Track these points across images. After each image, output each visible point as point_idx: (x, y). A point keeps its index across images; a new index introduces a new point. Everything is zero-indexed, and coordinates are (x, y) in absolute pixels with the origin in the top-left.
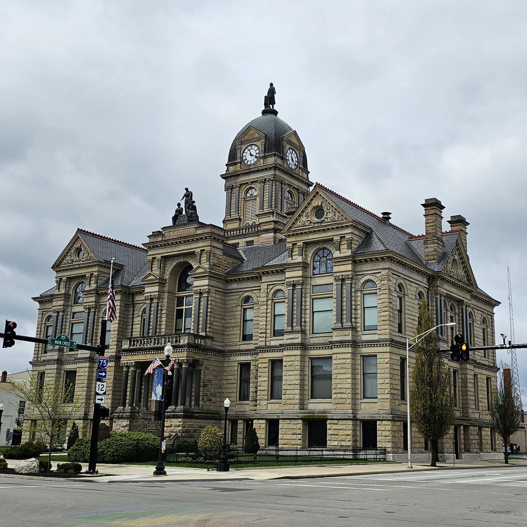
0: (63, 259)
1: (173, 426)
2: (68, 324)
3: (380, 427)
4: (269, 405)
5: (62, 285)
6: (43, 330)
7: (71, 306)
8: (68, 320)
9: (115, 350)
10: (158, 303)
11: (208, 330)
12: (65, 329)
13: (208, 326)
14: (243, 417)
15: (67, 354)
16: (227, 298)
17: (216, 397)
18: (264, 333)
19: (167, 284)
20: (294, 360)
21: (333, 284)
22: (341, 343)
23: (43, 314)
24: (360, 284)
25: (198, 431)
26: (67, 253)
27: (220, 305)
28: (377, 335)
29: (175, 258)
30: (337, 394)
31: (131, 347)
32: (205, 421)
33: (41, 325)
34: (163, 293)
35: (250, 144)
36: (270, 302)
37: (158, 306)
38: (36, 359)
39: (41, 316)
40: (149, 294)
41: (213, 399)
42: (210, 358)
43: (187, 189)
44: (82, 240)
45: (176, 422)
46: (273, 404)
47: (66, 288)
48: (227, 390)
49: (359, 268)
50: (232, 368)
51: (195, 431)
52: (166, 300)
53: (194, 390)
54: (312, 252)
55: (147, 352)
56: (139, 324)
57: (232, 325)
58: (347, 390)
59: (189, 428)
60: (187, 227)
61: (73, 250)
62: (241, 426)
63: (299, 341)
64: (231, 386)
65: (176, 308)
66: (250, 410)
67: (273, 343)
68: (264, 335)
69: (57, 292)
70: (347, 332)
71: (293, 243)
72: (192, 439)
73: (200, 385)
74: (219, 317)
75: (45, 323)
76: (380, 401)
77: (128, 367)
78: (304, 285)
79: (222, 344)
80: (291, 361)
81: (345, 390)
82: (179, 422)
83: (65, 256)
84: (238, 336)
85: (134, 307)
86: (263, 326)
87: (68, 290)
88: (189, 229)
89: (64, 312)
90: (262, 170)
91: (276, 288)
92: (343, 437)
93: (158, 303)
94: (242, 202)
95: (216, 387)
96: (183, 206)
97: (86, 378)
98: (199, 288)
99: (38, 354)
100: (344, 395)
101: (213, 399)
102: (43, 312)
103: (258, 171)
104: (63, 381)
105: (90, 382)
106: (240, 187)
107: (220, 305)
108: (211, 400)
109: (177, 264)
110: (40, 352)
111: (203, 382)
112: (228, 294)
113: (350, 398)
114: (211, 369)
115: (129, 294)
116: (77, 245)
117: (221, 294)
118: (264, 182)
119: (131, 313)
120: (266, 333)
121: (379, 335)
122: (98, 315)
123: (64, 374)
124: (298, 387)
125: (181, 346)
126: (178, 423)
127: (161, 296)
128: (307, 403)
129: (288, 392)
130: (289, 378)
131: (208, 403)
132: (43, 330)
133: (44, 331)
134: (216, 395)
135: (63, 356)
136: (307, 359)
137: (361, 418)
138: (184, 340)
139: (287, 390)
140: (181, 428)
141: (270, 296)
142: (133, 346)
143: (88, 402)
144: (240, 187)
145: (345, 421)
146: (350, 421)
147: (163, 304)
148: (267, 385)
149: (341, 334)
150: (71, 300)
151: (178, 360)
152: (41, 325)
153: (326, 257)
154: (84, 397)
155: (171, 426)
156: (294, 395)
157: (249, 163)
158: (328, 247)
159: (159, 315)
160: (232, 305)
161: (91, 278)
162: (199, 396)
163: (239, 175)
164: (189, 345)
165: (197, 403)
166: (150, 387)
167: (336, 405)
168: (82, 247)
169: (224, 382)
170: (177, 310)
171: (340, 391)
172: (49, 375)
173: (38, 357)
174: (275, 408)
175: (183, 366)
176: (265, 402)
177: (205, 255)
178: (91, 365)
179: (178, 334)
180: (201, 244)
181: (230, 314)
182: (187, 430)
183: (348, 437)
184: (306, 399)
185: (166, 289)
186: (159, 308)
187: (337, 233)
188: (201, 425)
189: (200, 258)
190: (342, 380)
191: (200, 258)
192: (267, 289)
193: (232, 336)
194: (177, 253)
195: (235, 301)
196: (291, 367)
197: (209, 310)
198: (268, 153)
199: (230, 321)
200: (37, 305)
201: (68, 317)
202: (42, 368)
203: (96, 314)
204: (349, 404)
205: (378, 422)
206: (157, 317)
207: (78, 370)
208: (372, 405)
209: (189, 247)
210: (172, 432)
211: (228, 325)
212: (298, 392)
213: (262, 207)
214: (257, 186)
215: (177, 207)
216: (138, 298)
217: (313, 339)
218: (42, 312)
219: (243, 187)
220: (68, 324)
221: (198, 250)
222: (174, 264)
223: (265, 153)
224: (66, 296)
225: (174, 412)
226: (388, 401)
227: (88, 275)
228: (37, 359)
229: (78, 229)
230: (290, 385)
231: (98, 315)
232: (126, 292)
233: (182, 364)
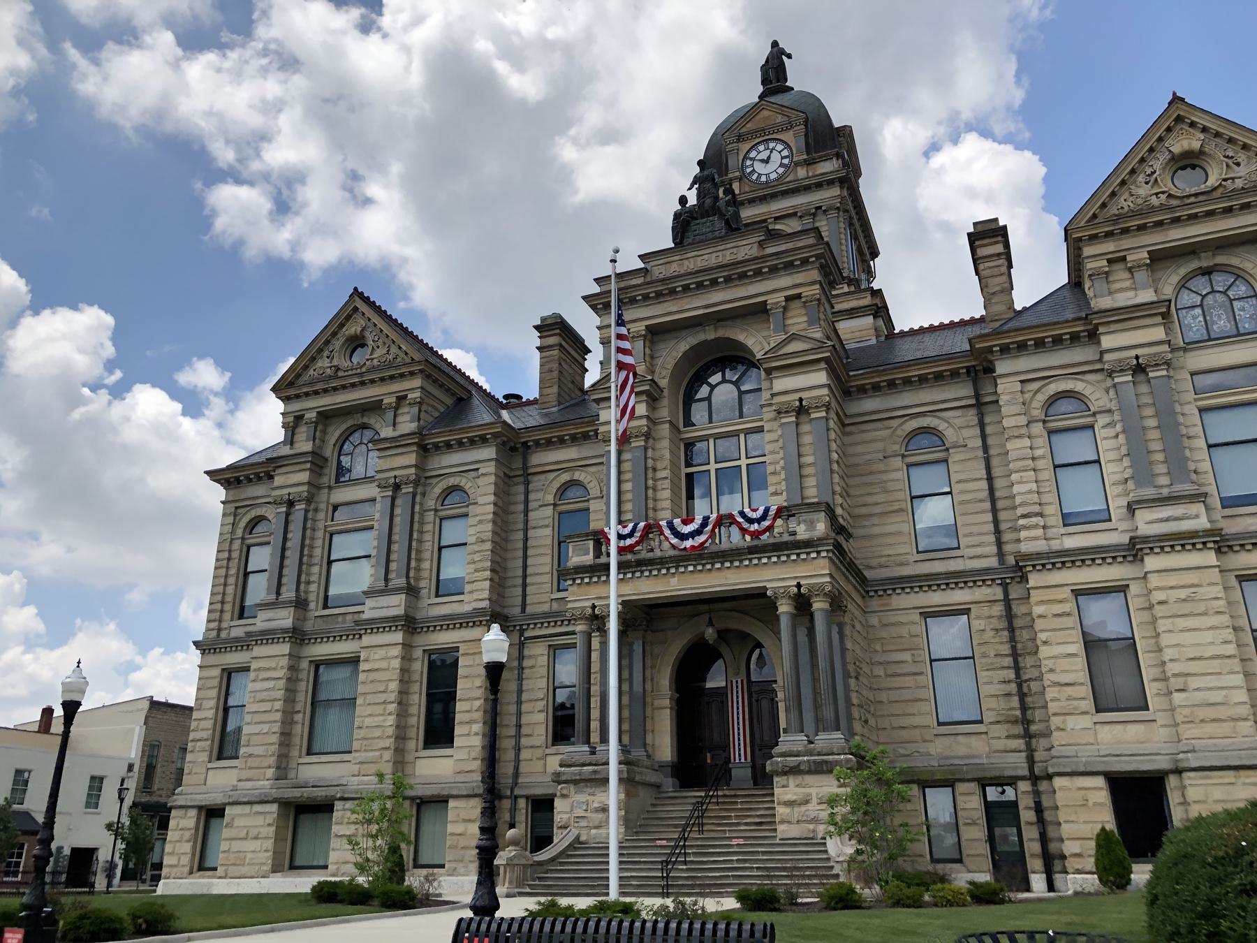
0: (306, 367)
1: (815, 800)
2: (320, 534)
5: (303, 432)
7: (330, 488)
8: (321, 525)
9: (486, 594)
12: (312, 547)
15: (317, 614)
19: (665, 402)
23: (235, 515)
26: (320, 350)
29: (684, 333)
33: (231, 543)
35: (761, 139)
36: (1038, 429)
38: (214, 633)
39: (231, 519)
46: (1119, 727)
47: (314, 440)
48: (894, 695)
55: (668, 569)
56: (547, 526)
57: (878, 509)
60: (729, 246)
61: (337, 344)
66: (995, 752)
67: (1071, 543)
69: (286, 451)
71: (1110, 256)
80: (1183, 587)
83: (313, 359)
85: (527, 483)
86: (1029, 496)
88: (735, 250)
97: (395, 675)
99: (220, 621)
102: (236, 508)
104: (307, 692)
109: (691, 348)
110: (227, 616)
118: (814, 215)
119: (522, 497)
122: (421, 504)
123: (309, 671)
129: (1194, 683)
130: (1189, 638)
132: (235, 555)
133: (240, 560)
135: (305, 619)
139: (1188, 675)
143: (401, 746)
150: (327, 471)
152: (231, 543)
154: (390, 731)
155: (807, 802)
156: (1224, 692)
158: (1235, 261)
160: (868, 457)
161: (396, 409)
168: (367, 334)
169: (879, 671)
173: (219, 630)
176: (1086, 721)
180: (784, 281)
185: (664, 412)
193: (891, 540)
198: (816, 152)
199: (870, 499)
201: (321, 515)
203: (418, 498)
207: (363, 656)
211: (859, 511)
217: (1239, 520)
218: (233, 508)
220: (320, 534)
221: (779, 298)
222: (684, 346)
223: (808, 153)
224: (317, 461)
227: (388, 400)
228: (218, 635)
229: (356, 289)
230: (1200, 658)
231: (421, 504)
232: (509, 440)
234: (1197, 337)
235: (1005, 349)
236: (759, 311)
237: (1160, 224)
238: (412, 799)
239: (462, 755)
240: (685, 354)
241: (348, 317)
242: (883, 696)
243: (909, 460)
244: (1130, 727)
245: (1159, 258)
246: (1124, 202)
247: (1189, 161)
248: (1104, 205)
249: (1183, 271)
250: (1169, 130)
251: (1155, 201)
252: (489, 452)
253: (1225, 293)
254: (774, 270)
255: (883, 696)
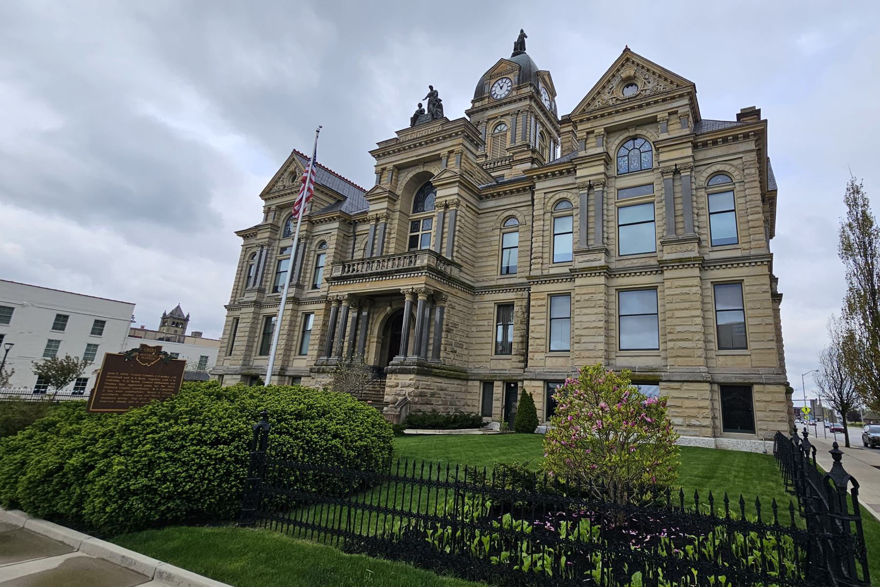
2: (273, 260)
3: (758, 395)
4: (549, 360)
6: (244, 269)
7: (279, 240)
8: (274, 256)
10: (386, 224)
11: (455, 254)
13: (456, 249)
14: (502, 378)
16: (480, 221)
17: (462, 348)
18: (539, 258)
19: (399, 202)
20: (594, 291)
21: (652, 184)
22: (679, 262)
24: (704, 179)
25: (437, 396)
27: (471, 227)
28: (740, 250)
30: (675, 340)
31: (345, 274)
32: (447, 381)
34: (393, 212)
36: (548, 216)
37: (385, 228)
39: (244, 253)
40: (375, 213)
41: (458, 350)
42: (457, 293)
43: (431, 87)
44: (298, 161)
45: (406, 379)
46: (555, 359)
47: (274, 218)
49: (700, 155)
50: (486, 311)
51: (433, 395)
52: (396, 221)
53: (432, 335)
54: (617, 142)
57: (487, 254)
58: (696, 335)
59: (425, 390)
61: (286, 174)
62: (499, 390)
63: (602, 263)
64: (484, 334)
65: (410, 234)
67: (552, 271)
68: (540, 260)
70: (690, 246)
72: (429, 406)
73: (442, 328)
74: (470, 242)
75: (248, 262)
76: (755, 353)
77: (339, 302)
78: (606, 188)
79: (472, 279)
81: (691, 334)
82: (410, 380)
83: (277, 182)
84: (495, 268)
87: (278, 222)
89: (269, 245)
90: (515, 101)
91: (557, 197)
92: (692, 410)
93: (386, 224)
94: (490, 138)
95: (462, 334)
96: (425, 106)
98: (444, 199)
100: (690, 342)
101: (458, 350)
103: (510, 103)
105: (292, 328)
106: (487, 122)
107: (471, 227)
108: (455, 352)
110: (238, 295)
111: (447, 325)
112: (481, 216)
113: (701, 348)
114: (457, 308)
115: (350, 224)
116: (292, 168)
117: (473, 213)
119: (352, 246)
120: (542, 258)
121: (744, 249)
122: (309, 248)
124: (602, 332)
125: (418, 269)
126: (409, 382)
127: (391, 216)
128: (614, 357)
129: (584, 339)
130: (585, 318)
131: (452, 355)
132: (244, 269)
134: (463, 345)
136: (613, 291)
137: (723, 381)
138: (422, 261)
140: (411, 389)
141: (549, 208)
142: (348, 273)
144: (487, 122)
145: (695, 385)
146: (707, 384)
147: (393, 226)
148: (545, 330)
149: (679, 249)
150: (279, 232)
151: (413, 288)
153: (639, 149)
156: (594, 345)
157: (499, 97)
158: (644, 133)
159: (386, 240)
162: (440, 344)
163: (487, 109)
164: (430, 268)
165: (437, 355)
166: (369, 332)
167: (674, 359)
168: (297, 170)
169: (474, 329)
170: (411, 237)
171: (680, 336)
172: (244, 321)
173: (235, 301)
174: (558, 364)
175: (420, 298)
176: (542, 356)
177: (455, 158)
178: (296, 307)
179: (414, 252)
180: (449, 143)
181: (484, 240)
182: (421, 392)
183: (703, 411)
184: (613, 351)
185: (398, 207)
186: (387, 230)
187: (664, 108)
188: (441, 387)
189: (447, 162)
190: (684, 320)
191: (447, 162)
192: (544, 198)
194: (415, 158)
195: (492, 224)
196: (589, 302)
197: (457, 228)
200: (241, 241)
201: (275, 252)
202: (236, 313)
203: (307, 245)
204: (700, 357)
205: (756, 388)
206: (383, 242)
208: (739, 359)
209: (432, 149)
210: (399, 395)
212: (602, 339)
213: (513, 140)
214: (508, 120)
215: (418, 108)
216: (361, 228)
217: (623, 262)
218: (246, 248)
219: (491, 122)
220: (273, 260)
221: (445, 152)
222: (410, 175)
224: (274, 228)
225: (402, 364)
226: (772, 353)
229: (294, 150)
231: (309, 248)
233: (417, 294)
234: (624, 171)
235: (539, 177)
236: (437, 159)
237: (610, 114)
238: (290, 376)
239: (309, 358)
240: (411, 178)
241: (291, 162)
242: (473, 341)
243: (503, 231)
244: (560, 359)
245: (610, 131)
246: (597, 104)
247: (629, 82)
248: (589, 104)
249: (621, 138)
250: (623, 65)
251: (611, 103)
252: (336, 225)
253: (639, 149)
254: (444, 138)
255: (473, 341)
